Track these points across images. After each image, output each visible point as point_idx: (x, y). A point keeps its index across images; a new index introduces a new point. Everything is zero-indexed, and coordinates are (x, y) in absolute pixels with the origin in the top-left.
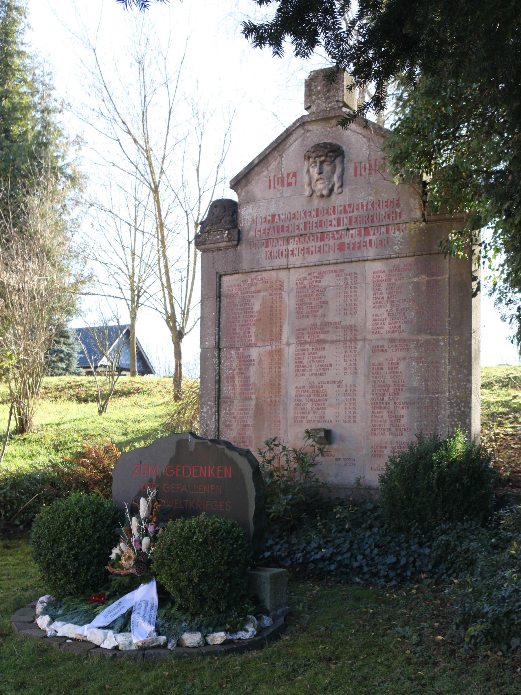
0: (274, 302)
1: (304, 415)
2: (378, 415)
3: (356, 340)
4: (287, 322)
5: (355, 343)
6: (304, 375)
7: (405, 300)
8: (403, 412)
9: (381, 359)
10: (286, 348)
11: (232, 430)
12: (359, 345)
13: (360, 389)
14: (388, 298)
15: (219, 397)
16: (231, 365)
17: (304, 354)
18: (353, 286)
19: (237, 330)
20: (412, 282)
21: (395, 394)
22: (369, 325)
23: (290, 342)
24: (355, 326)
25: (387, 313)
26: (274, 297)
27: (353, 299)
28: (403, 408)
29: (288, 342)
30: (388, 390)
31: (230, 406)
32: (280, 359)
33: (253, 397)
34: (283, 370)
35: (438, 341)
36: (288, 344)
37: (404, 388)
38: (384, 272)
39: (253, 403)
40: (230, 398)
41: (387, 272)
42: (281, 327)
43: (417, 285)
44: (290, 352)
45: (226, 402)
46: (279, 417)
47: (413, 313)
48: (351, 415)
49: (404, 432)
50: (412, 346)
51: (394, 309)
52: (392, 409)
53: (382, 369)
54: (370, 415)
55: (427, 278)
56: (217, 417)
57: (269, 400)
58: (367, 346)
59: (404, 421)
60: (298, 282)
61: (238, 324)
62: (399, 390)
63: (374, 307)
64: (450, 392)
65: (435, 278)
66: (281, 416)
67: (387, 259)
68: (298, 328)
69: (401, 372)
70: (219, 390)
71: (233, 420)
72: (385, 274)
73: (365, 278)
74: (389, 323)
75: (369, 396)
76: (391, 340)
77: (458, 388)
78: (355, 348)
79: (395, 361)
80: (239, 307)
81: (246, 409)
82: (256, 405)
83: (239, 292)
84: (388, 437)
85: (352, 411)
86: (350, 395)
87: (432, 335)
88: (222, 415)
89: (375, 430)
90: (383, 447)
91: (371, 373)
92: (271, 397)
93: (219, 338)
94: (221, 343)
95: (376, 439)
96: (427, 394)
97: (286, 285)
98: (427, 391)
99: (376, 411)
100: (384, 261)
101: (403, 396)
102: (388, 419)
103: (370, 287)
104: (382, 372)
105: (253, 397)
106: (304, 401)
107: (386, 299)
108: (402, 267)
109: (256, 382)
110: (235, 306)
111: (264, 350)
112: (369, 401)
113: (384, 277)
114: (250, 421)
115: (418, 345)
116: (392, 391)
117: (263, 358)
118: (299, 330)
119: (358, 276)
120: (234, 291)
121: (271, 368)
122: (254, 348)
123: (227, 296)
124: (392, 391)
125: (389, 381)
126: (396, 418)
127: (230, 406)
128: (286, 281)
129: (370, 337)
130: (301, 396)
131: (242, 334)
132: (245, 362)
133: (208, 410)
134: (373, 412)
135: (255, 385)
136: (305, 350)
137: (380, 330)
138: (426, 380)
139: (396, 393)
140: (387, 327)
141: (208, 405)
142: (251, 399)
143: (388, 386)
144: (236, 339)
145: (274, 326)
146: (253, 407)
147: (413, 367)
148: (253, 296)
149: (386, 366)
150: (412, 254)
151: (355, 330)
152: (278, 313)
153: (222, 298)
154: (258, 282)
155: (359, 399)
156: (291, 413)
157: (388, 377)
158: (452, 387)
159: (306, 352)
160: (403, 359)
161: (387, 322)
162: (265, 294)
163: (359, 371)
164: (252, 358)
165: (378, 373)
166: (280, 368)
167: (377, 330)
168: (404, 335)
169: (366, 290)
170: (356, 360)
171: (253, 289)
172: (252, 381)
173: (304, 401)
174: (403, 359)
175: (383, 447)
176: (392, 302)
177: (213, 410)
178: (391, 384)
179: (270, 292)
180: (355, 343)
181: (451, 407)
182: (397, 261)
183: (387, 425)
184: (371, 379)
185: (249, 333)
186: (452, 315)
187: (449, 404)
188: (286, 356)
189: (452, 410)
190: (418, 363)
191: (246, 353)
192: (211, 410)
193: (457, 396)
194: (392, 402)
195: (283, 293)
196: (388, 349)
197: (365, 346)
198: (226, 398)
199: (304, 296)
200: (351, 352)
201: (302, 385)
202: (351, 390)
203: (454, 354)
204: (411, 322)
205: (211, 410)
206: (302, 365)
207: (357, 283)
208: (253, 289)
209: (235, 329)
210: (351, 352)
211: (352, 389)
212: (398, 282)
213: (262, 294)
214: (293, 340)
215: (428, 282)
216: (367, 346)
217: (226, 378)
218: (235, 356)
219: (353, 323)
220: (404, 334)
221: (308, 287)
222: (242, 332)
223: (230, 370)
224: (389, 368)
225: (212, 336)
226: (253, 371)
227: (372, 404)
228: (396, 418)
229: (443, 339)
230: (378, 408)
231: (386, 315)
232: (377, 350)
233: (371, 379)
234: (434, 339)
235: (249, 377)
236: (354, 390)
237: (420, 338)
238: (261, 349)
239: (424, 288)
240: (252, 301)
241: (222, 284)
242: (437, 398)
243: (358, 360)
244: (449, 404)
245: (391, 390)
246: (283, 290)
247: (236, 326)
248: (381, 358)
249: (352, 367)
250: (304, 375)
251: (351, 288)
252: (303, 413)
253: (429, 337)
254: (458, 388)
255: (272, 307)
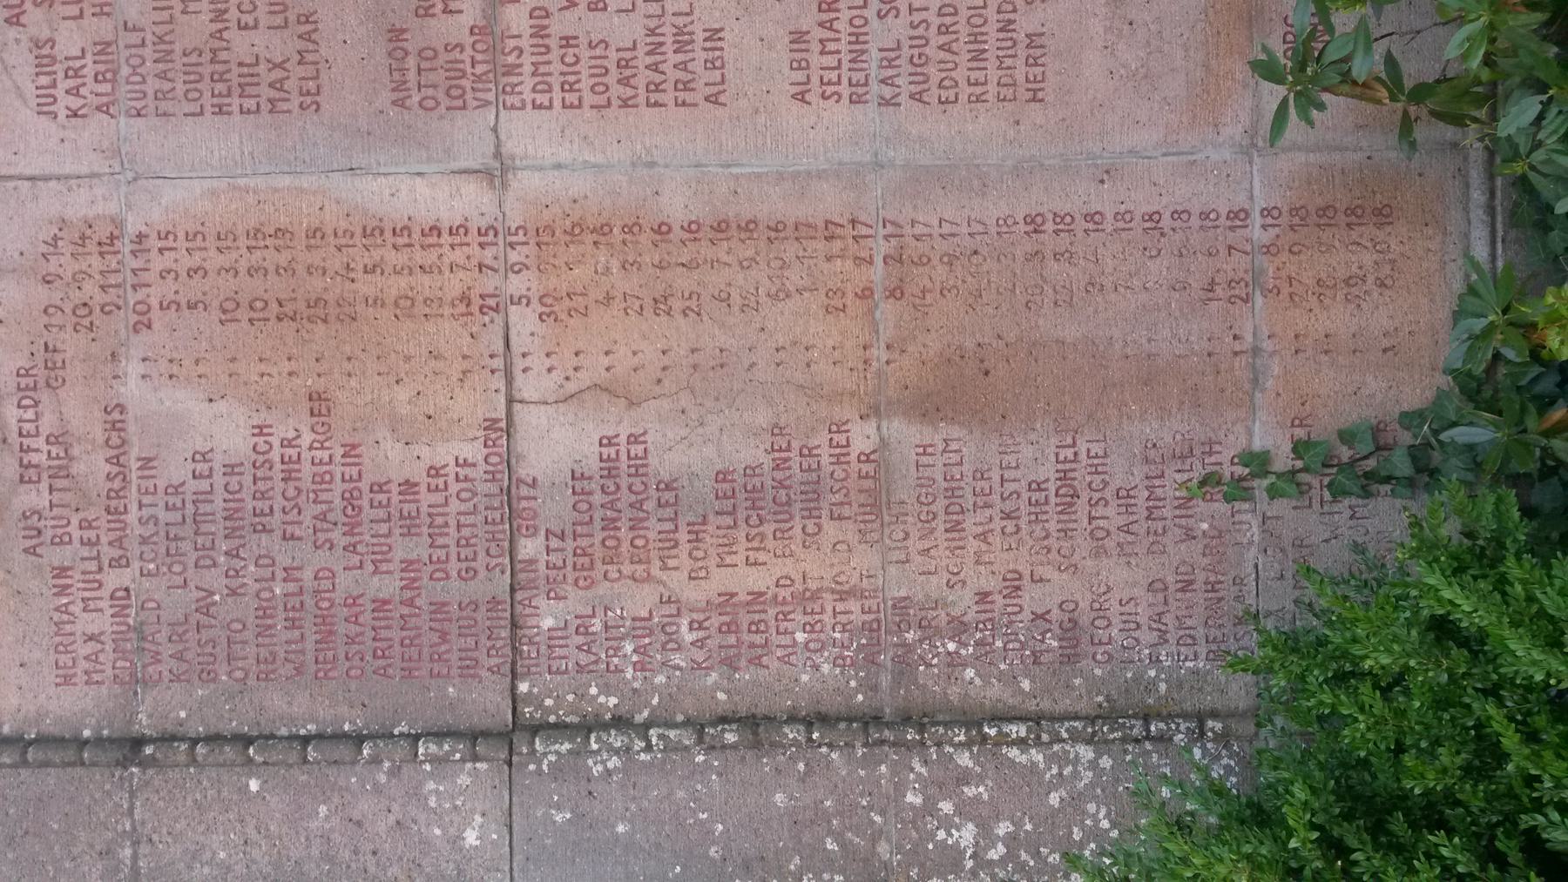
0: (193, 289)
1: (992, 28)
4: (341, 185)
6: (714, 34)
10: (526, 183)
11: (1100, 611)
15: (871, 719)
16: (642, 626)
17: (567, 41)
19: (388, 586)
23: (477, 153)
26: (154, 295)
29: (485, 174)
31: (929, 631)
32: (603, 230)
33: (863, 437)
34: (676, 205)
36: (497, 173)
39: (905, 433)
40: (871, 629)
42: (373, 232)
44: (557, 155)
45: (905, 665)
46: (1005, 221)
56: (1017, 730)
57: (887, 311)
60: (64, 102)
61: (345, 581)
66: (992, 210)
68: (385, 97)
70: (817, 719)
71: (1032, 599)
80: (214, 579)
81: (951, 493)
82: (928, 406)
83: (113, 579)
88: (995, 693)
92: (866, 294)
93: (439, 735)
94: (479, 721)
97: (81, 205)
105: (863, 437)
106: (898, 28)
109: (763, 418)
110: (206, 609)
111: (537, 362)
114: (1036, 456)
117: (594, 369)
118: (400, 86)
120: (102, 623)
121: (661, 304)
122: (522, 444)
123: (135, 682)
127: (929, 631)
128: (50, 203)
130: (857, 57)
131: (418, 549)
132: (623, 504)
133: (966, 810)
135: (777, 430)
136: (540, 32)
141: (929, 808)
142: (876, 458)
144: (454, 590)
145: (366, 286)
146: (935, 436)
148: (146, 463)
152: (272, 258)
153: (144, 723)
154: (48, 424)
156: (975, 131)
159: (559, 26)
162: (134, 368)
164: (589, 455)
166: (662, 230)
171: (92, 466)
172: (750, 453)
173: (898, 28)
177: (965, 759)
179: (121, 322)
185: (409, 486)
188: (579, 184)
191: (555, 509)
192: (964, 778)
195: (133, 226)
198: (871, 661)
199: (165, 57)
201: (781, 54)
205: (964, 778)
206: (643, 60)
208: (92, 466)
209: (381, 604)
213: (132, 389)
214: (469, 136)
217: (731, 664)
218: (575, 601)
221: (104, 28)
222: (403, 549)
223: (672, 642)
225: (416, 795)
226: (685, 450)
235: (722, 476)
238: (527, 387)
240: (175, 470)
241: (49, 727)
246: (117, 222)
247: (353, 601)
250: (714, 34)
252: (975, 38)
255: (227, 315)
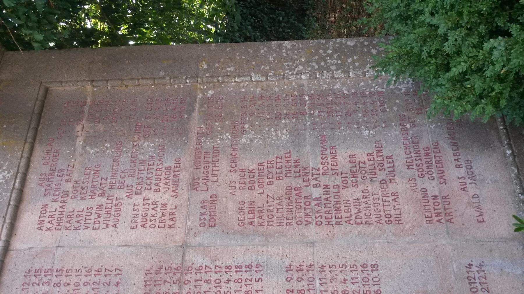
2: (354, 211)
3: (183, 269)
5: (189, 270)
7: (115, 160)
8: (343, 157)
9: (230, 206)
12: (196, 259)
13: (299, 255)
14: (102, 195)
18: (55, 280)
20: (84, 148)
21: (306, 174)
22: (151, 236)
24: (148, 272)
25: (135, 197)
27: (84, 279)
28: (334, 158)
30: (296, 189)
35: (206, 100)
37: (294, 157)
38: (45, 206)
41: (47, 200)
43: (92, 139)
47: (146, 144)
48: (361, 276)
49: (385, 153)
50: (209, 143)
51: (129, 181)
52: (338, 180)
53: (251, 203)
54: (355, 229)
55: (83, 122)
58: (199, 239)
59: (361, 155)
62: (296, 166)
63: (115, 226)
64: (300, 73)
65: (86, 109)
67: (20, 200)
69: (261, 164)
72: (50, 204)
73: (45, 250)
74: (157, 191)
75: (313, 232)
76: (194, 186)
77: (293, 60)
78: (199, 270)
79: (236, 177)
84: (400, 186)
85: (350, 276)
86: (312, 280)
87: (193, 110)
89: (389, 216)
90: (425, 196)
91: (261, 229)
95: (410, 213)
96: (304, 114)
98: (299, 114)
99: (345, 215)
100: (22, 207)
101: (312, 159)
102: (361, 187)
103: (69, 237)
104: (258, 204)
107: (103, 200)
108: (46, 169)
112: (325, 230)
113: (57, 205)
115: (209, 132)
116: (300, 181)
119: (37, 266)
124: (300, 181)
125: (277, 188)
126: (357, 170)
129: (179, 235)
134: (348, 222)
137: (168, 211)
138: (278, 117)
139: (304, 173)
140: (164, 197)
143: (289, 189)
147: (252, 140)
149: (246, 196)
150: (27, 146)
151: (158, 272)
155: (320, 256)
157: (270, 190)
158: (290, 69)
160: (234, 160)
161: (152, 196)
163: (256, 258)
165: (261, 212)
167: (168, 217)
168: (187, 160)
169: (71, 247)
170: (228, 267)
174: (234, 160)
175: (425, 196)
176: (112, 187)
178: (285, 182)
180: (189, 270)
181: (328, 69)
182: (33, 179)
183: (374, 188)
184: (274, 227)
186: (161, 74)
187: (321, 74)
189: (333, 67)
190: (243, 131)
193: (307, 62)
194: (324, 180)
196: (210, 192)
197: (199, 245)
200: (207, 281)
202: (300, 279)
203: (232, 69)
204: (162, 148)
207: (51, 270)
210: (207, 281)
211: (296, 275)
212: (75, 176)
215: (92, 119)
216: (199, 239)
219: (139, 278)
220: (183, 161)
224: (250, 188)
227: (329, 224)
228: (357, 170)
229: (202, 91)
230: (338, 209)
231: (138, 199)
232: (210, 219)
233: (274, 227)
234: (202, 106)
236: (299, 269)
237: (196, 130)
239: (101, 127)
242: (311, 96)
243: (229, 263)
244: (321, 74)
245: (299, 183)
248: (228, 207)
249: (246, 276)
251: (56, 285)
253: (196, 115)
254: (293, 60)
